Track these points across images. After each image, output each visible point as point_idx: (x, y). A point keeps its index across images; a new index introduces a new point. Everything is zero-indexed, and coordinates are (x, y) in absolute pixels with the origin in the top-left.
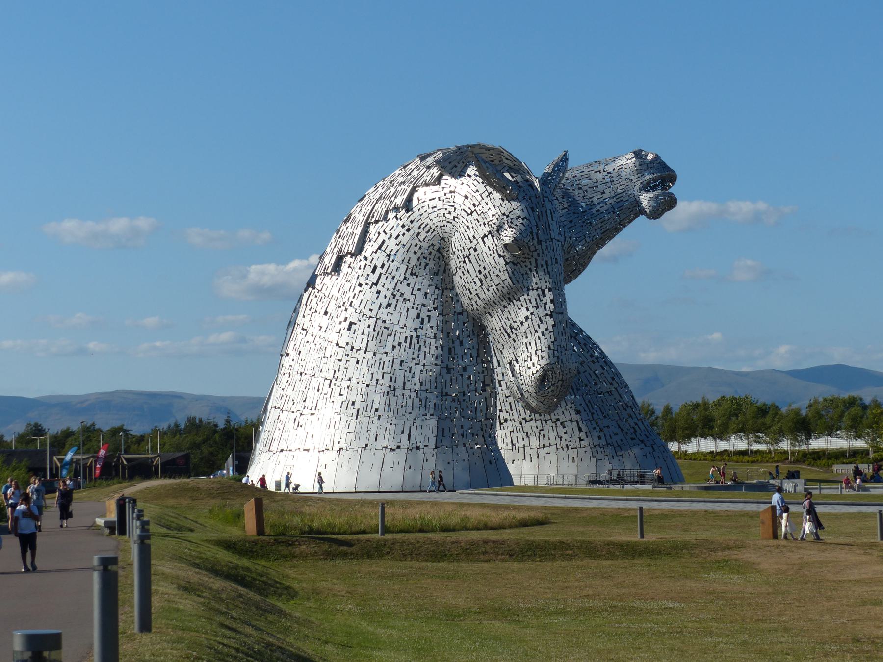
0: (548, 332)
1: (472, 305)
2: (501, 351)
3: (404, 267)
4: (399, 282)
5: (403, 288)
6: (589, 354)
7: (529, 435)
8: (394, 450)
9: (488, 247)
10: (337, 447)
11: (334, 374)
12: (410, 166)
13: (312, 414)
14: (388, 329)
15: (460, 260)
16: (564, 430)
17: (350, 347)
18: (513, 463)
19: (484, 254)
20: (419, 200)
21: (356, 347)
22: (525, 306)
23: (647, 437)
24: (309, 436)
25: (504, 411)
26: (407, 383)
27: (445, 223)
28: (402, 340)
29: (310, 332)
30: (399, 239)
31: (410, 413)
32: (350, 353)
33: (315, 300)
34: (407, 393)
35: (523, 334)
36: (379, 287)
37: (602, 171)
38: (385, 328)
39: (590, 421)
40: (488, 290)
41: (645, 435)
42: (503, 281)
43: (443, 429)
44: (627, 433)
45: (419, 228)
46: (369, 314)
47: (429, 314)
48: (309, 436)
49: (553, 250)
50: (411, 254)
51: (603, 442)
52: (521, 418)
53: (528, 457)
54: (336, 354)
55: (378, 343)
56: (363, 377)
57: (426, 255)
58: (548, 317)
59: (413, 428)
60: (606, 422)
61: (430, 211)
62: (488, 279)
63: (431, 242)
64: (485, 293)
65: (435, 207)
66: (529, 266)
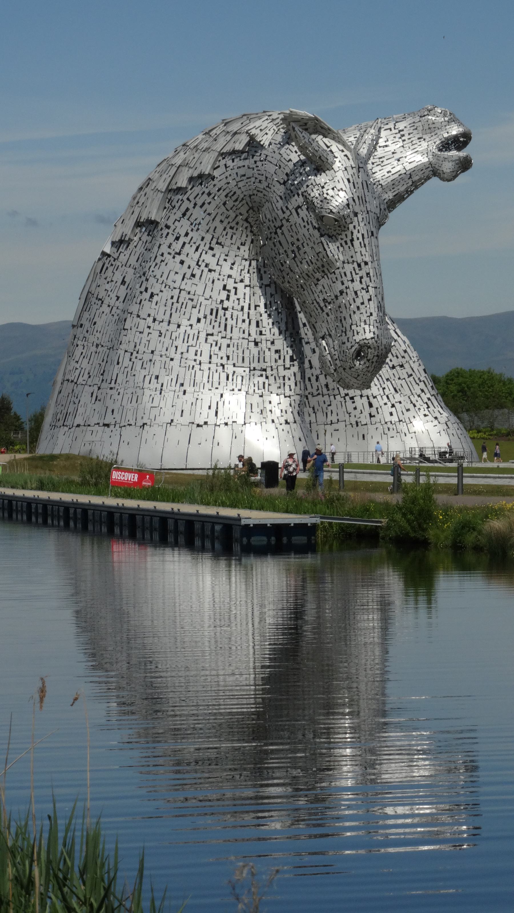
0: (363, 306)
2: (313, 325)
3: (208, 237)
4: (204, 252)
5: (208, 258)
7: (316, 410)
8: (201, 426)
9: (302, 218)
10: (140, 423)
11: (135, 346)
12: (214, 131)
13: (111, 388)
14: (192, 300)
15: (271, 230)
16: (354, 405)
17: (151, 319)
19: (297, 225)
20: (226, 167)
21: (159, 318)
22: (340, 279)
23: (441, 414)
24: (109, 411)
26: (214, 357)
27: (255, 192)
28: (208, 312)
29: (106, 302)
30: (204, 208)
31: (217, 388)
32: (151, 324)
33: (111, 269)
34: (213, 367)
35: (337, 309)
36: (183, 257)
37: (393, 129)
38: (189, 299)
40: (301, 263)
42: (317, 254)
43: (251, 404)
44: (419, 409)
45: (226, 196)
46: (172, 285)
47: (236, 285)
48: (109, 411)
49: (369, 223)
50: (217, 223)
51: (395, 418)
54: (136, 326)
55: (182, 315)
56: (167, 350)
57: (233, 224)
58: (364, 292)
59: (220, 404)
61: (238, 179)
62: (301, 252)
63: (238, 212)
64: (298, 266)
65: (244, 175)
66: (345, 239)
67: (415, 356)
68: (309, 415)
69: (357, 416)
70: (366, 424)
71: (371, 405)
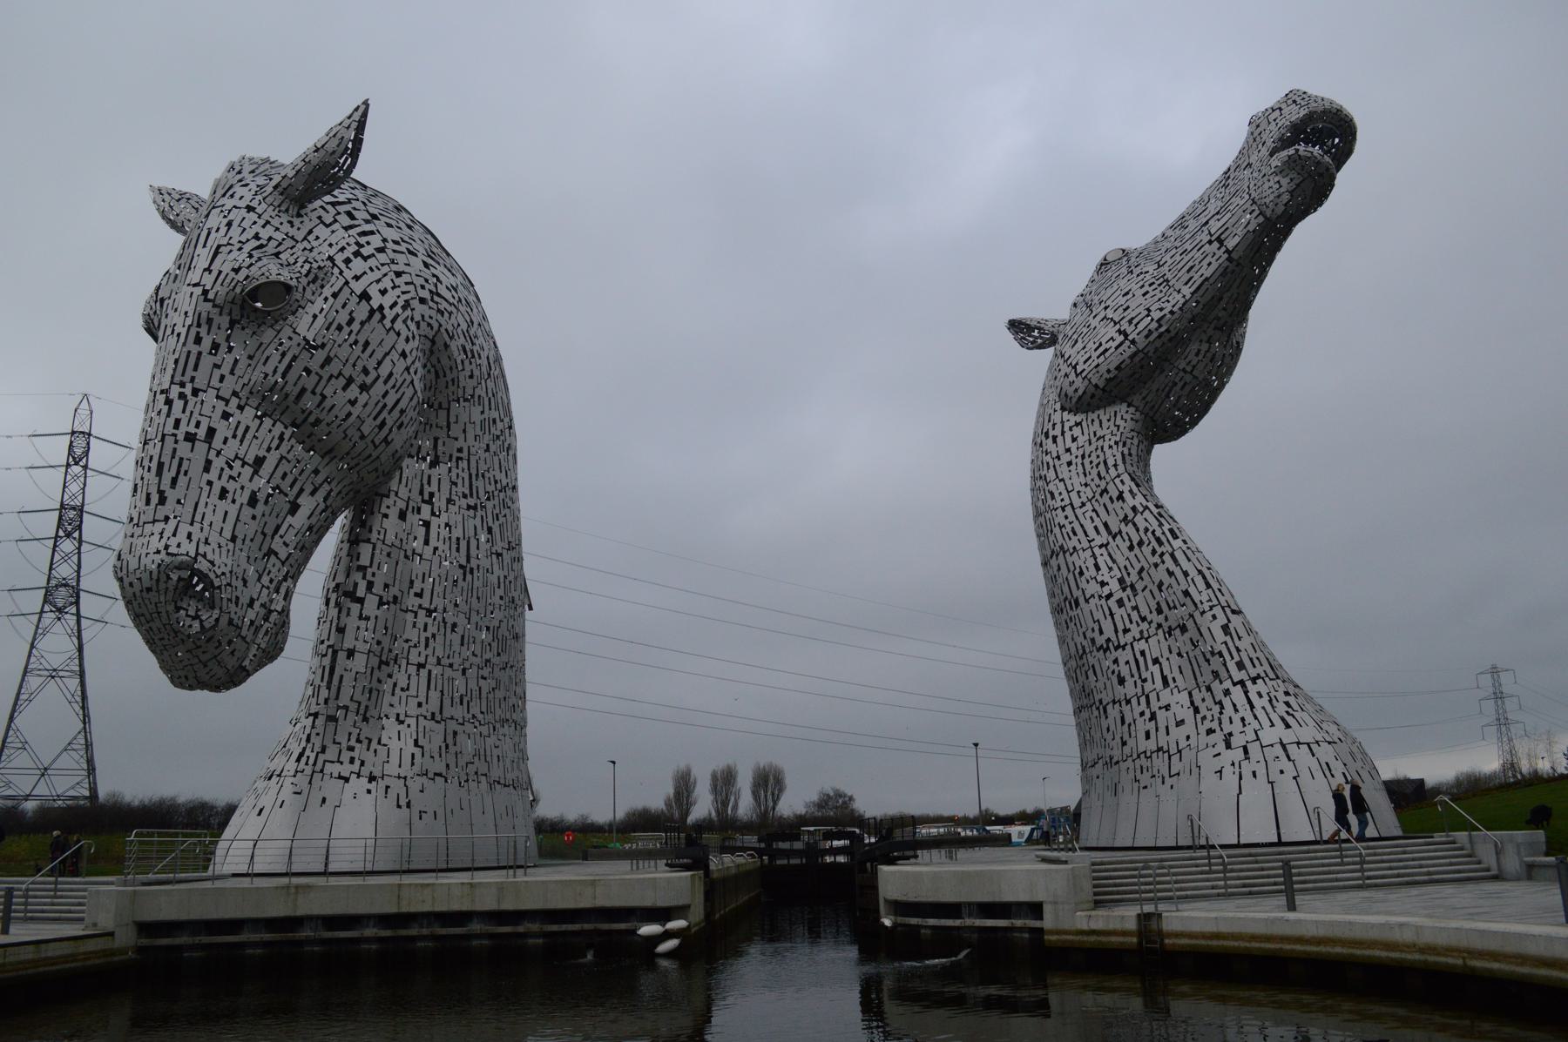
6: (1150, 547)
39: (1138, 698)
41: (1243, 719)
44: (1204, 718)
49: (176, 310)
60: (1166, 696)
67: (1205, 598)
70: (1117, 762)
71: (1123, 722)
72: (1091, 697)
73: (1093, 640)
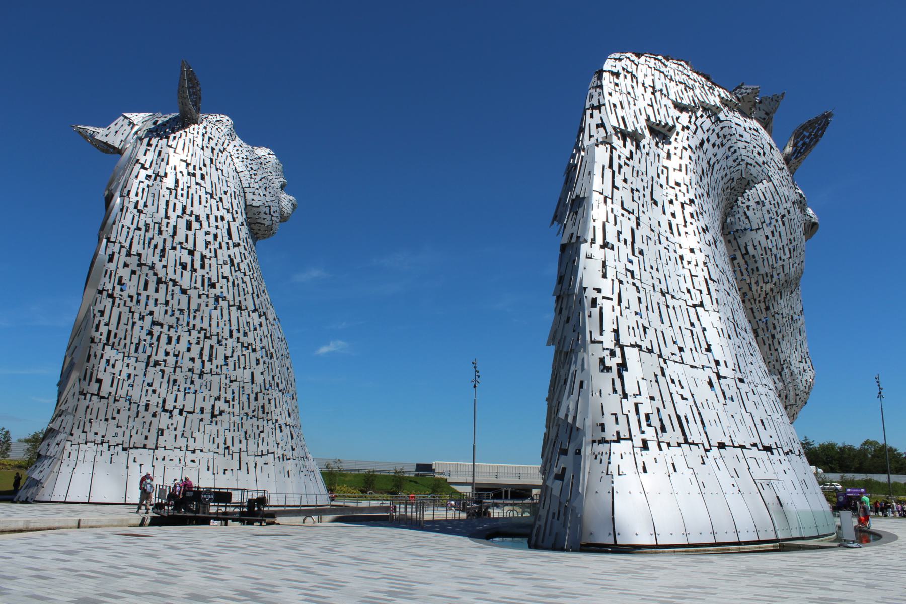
1: (772, 277)
18: (225, 473)
25: (223, 400)
52: (242, 412)
53: (244, 467)
68: (240, 442)
69: (284, 449)
72: (270, 415)
73: (278, 384)
